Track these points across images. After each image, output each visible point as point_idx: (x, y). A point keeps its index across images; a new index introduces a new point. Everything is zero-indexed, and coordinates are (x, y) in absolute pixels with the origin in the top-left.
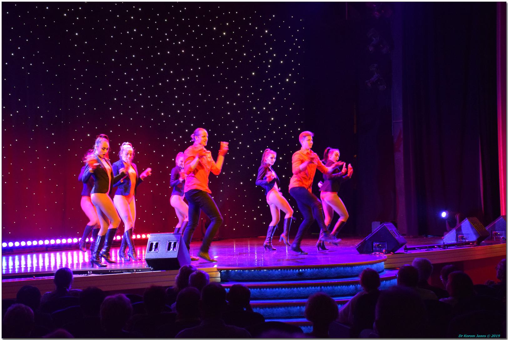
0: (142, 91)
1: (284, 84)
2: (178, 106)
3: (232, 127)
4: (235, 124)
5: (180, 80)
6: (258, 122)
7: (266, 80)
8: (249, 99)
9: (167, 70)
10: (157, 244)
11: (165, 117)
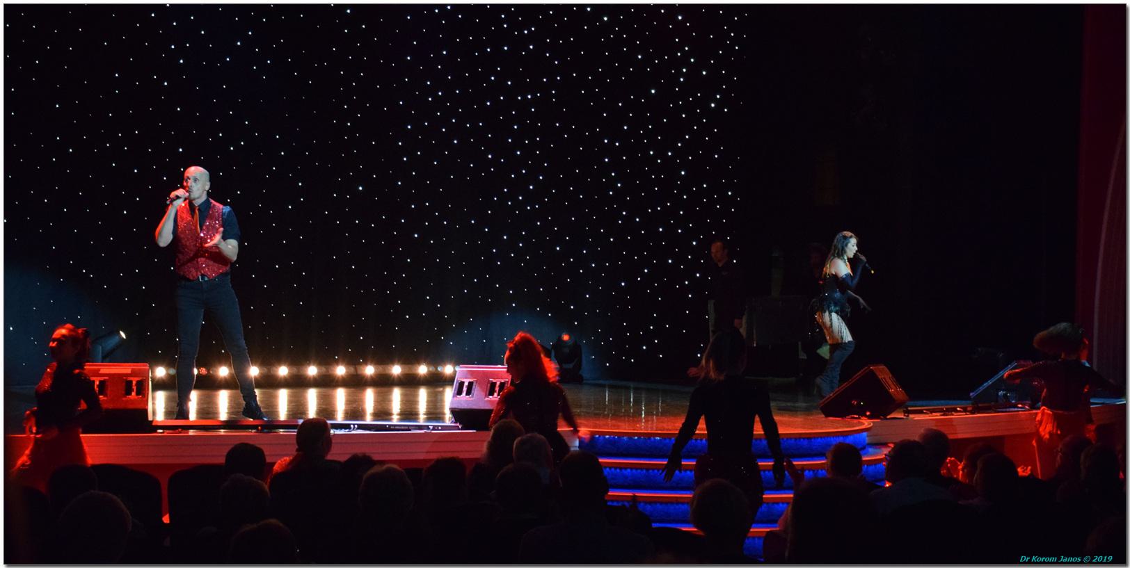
0: (457, 115)
1: (706, 111)
2: (518, 144)
3: (611, 184)
4: (616, 180)
5: (525, 97)
6: (658, 177)
7: (676, 104)
8: (643, 136)
9: (502, 77)
10: (471, 384)
11: (494, 162)
